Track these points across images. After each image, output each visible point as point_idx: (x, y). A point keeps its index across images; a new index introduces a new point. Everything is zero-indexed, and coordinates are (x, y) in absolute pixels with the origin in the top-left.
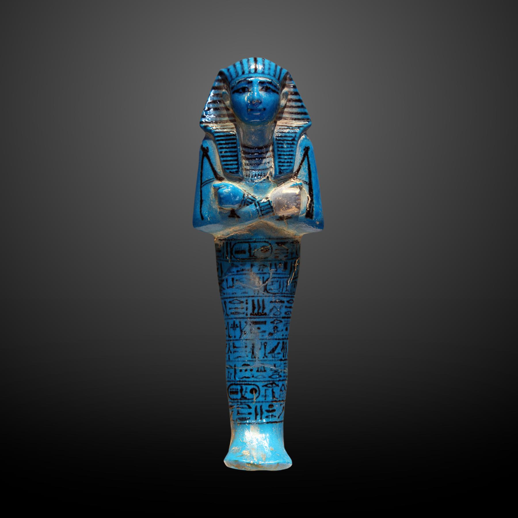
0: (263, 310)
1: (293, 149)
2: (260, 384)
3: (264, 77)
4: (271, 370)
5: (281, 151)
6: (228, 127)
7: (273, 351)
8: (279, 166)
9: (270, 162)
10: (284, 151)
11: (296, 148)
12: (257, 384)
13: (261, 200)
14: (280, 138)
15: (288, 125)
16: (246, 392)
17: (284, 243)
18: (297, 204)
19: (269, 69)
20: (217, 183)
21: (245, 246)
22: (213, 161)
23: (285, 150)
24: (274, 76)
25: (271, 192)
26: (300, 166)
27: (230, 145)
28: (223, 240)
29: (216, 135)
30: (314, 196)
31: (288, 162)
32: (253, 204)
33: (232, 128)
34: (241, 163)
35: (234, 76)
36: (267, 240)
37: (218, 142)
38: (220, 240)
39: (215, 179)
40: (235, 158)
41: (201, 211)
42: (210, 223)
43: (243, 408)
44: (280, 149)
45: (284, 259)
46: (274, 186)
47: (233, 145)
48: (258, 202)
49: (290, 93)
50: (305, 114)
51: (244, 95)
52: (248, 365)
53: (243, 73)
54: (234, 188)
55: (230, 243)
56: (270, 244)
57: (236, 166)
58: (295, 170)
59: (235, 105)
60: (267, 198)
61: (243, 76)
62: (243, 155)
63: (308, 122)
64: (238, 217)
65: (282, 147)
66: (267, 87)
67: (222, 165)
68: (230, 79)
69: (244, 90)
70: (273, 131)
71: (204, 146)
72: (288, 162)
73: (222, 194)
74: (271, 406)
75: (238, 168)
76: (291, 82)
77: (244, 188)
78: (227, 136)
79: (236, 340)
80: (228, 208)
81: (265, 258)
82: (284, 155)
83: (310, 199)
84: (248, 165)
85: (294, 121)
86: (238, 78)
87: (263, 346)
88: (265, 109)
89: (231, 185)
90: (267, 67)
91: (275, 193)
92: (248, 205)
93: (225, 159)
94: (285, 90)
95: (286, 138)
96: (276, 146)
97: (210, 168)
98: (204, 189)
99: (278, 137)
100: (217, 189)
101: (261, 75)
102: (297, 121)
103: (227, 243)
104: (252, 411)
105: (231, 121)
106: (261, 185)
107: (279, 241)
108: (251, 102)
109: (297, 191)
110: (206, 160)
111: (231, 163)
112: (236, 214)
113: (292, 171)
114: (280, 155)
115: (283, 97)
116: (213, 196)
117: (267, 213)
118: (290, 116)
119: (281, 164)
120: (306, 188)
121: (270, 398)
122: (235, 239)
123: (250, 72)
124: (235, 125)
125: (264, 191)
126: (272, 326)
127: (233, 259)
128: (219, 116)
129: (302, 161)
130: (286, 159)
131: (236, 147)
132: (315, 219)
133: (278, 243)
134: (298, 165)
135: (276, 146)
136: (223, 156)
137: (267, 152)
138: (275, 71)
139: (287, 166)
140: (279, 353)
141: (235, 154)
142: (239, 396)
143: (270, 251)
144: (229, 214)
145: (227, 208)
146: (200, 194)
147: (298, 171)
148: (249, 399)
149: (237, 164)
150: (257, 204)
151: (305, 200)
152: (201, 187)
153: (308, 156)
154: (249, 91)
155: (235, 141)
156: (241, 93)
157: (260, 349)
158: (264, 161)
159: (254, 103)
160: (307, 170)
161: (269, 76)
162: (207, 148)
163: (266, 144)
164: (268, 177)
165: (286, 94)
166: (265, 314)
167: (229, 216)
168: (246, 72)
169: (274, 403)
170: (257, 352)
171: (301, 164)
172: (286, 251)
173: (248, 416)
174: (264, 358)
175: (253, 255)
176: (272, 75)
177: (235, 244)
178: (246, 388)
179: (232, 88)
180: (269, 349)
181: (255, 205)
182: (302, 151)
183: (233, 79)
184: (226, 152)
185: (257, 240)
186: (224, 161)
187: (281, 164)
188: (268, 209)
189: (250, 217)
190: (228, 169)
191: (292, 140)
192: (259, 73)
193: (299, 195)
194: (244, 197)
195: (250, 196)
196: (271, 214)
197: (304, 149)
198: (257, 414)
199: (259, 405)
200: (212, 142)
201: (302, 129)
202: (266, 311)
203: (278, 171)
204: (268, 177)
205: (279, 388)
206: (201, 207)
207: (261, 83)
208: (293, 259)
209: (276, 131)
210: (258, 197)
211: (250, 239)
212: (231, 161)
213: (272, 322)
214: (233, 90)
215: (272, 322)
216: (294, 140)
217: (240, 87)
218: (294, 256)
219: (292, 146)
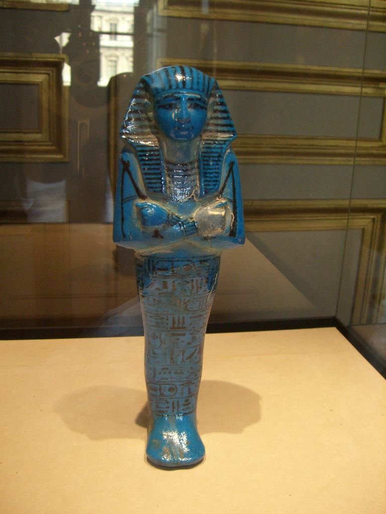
0: (182, 325)
2: (177, 384)
3: (193, 93)
4: (188, 372)
8: (205, 185)
10: (210, 169)
11: (222, 165)
12: (175, 383)
14: (206, 155)
16: (164, 390)
17: (205, 261)
19: (198, 83)
20: (140, 202)
22: (134, 177)
23: (211, 167)
24: (203, 90)
25: (196, 212)
30: (238, 214)
31: (214, 181)
36: (190, 259)
38: (141, 255)
41: (122, 229)
43: (161, 403)
50: (231, 126)
51: (171, 112)
52: (167, 369)
55: (153, 261)
60: (192, 218)
61: (170, 91)
64: (162, 237)
65: (208, 165)
66: (196, 104)
69: (170, 107)
71: (124, 159)
72: (214, 181)
73: (147, 216)
74: (187, 401)
79: (156, 348)
80: (151, 229)
82: (210, 173)
83: (234, 217)
85: (219, 134)
87: (181, 353)
89: (155, 205)
90: (195, 80)
93: (148, 176)
95: (212, 155)
98: (125, 205)
99: (204, 153)
100: (141, 209)
101: (190, 91)
103: (149, 260)
104: (170, 405)
105: (153, 133)
107: (201, 259)
108: (178, 121)
110: (126, 175)
111: (156, 181)
112: (159, 235)
114: (206, 173)
123: (178, 87)
124: (158, 139)
125: (190, 211)
128: (141, 127)
130: (211, 177)
133: (201, 262)
135: (202, 164)
136: (146, 174)
138: (204, 85)
139: (214, 185)
142: (158, 393)
144: (152, 234)
146: (121, 211)
147: (223, 188)
148: (167, 396)
152: (122, 204)
153: (232, 171)
154: (176, 108)
156: (167, 109)
157: (178, 355)
160: (231, 186)
161: (197, 92)
162: (128, 161)
163: (191, 159)
164: (193, 197)
166: (185, 328)
167: (153, 236)
168: (174, 87)
171: (226, 181)
172: (208, 268)
174: (181, 362)
176: (201, 90)
177: (158, 262)
178: (165, 387)
179: (158, 102)
184: (149, 169)
186: (148, 179)
187: (207, 183)
188: (192, 230)
189: (174, 236)
194: (168, 217)
195: (174, 217)
196: (196, 234)
197: (229, 165)
198: (174, 408)
199: (176, 401)
204: (193, 197)
206: (122, 224)
207: (190, 99)
212: (154, 179)
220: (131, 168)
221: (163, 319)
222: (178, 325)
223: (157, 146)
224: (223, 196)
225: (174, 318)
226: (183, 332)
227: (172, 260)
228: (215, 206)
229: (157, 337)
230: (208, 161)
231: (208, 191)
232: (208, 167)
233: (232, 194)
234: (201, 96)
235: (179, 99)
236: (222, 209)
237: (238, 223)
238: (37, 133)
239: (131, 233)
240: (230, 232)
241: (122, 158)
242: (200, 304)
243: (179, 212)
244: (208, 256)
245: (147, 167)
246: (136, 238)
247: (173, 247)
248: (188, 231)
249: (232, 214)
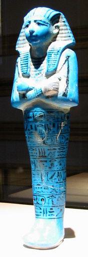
2: (46, 196)
7: (52, 178)
9: (44, 65)
30: (69, 84)
40: (26, 65)
104: (42, 211)
121: (51, 205)
126: (50, 163)
133: (48, 112)
134: (61, 66)
140: (55, 179)
169: (53, 208)
170: (43, 178)
173: (40, 214)
180: (50, 176)
202: (46, 155)
205: (56, 199)
208: (58, 121)
213: (50, 161)
215: (50, 161)
226: (45, 160)
237: (69, 89)
242: (52, 140)
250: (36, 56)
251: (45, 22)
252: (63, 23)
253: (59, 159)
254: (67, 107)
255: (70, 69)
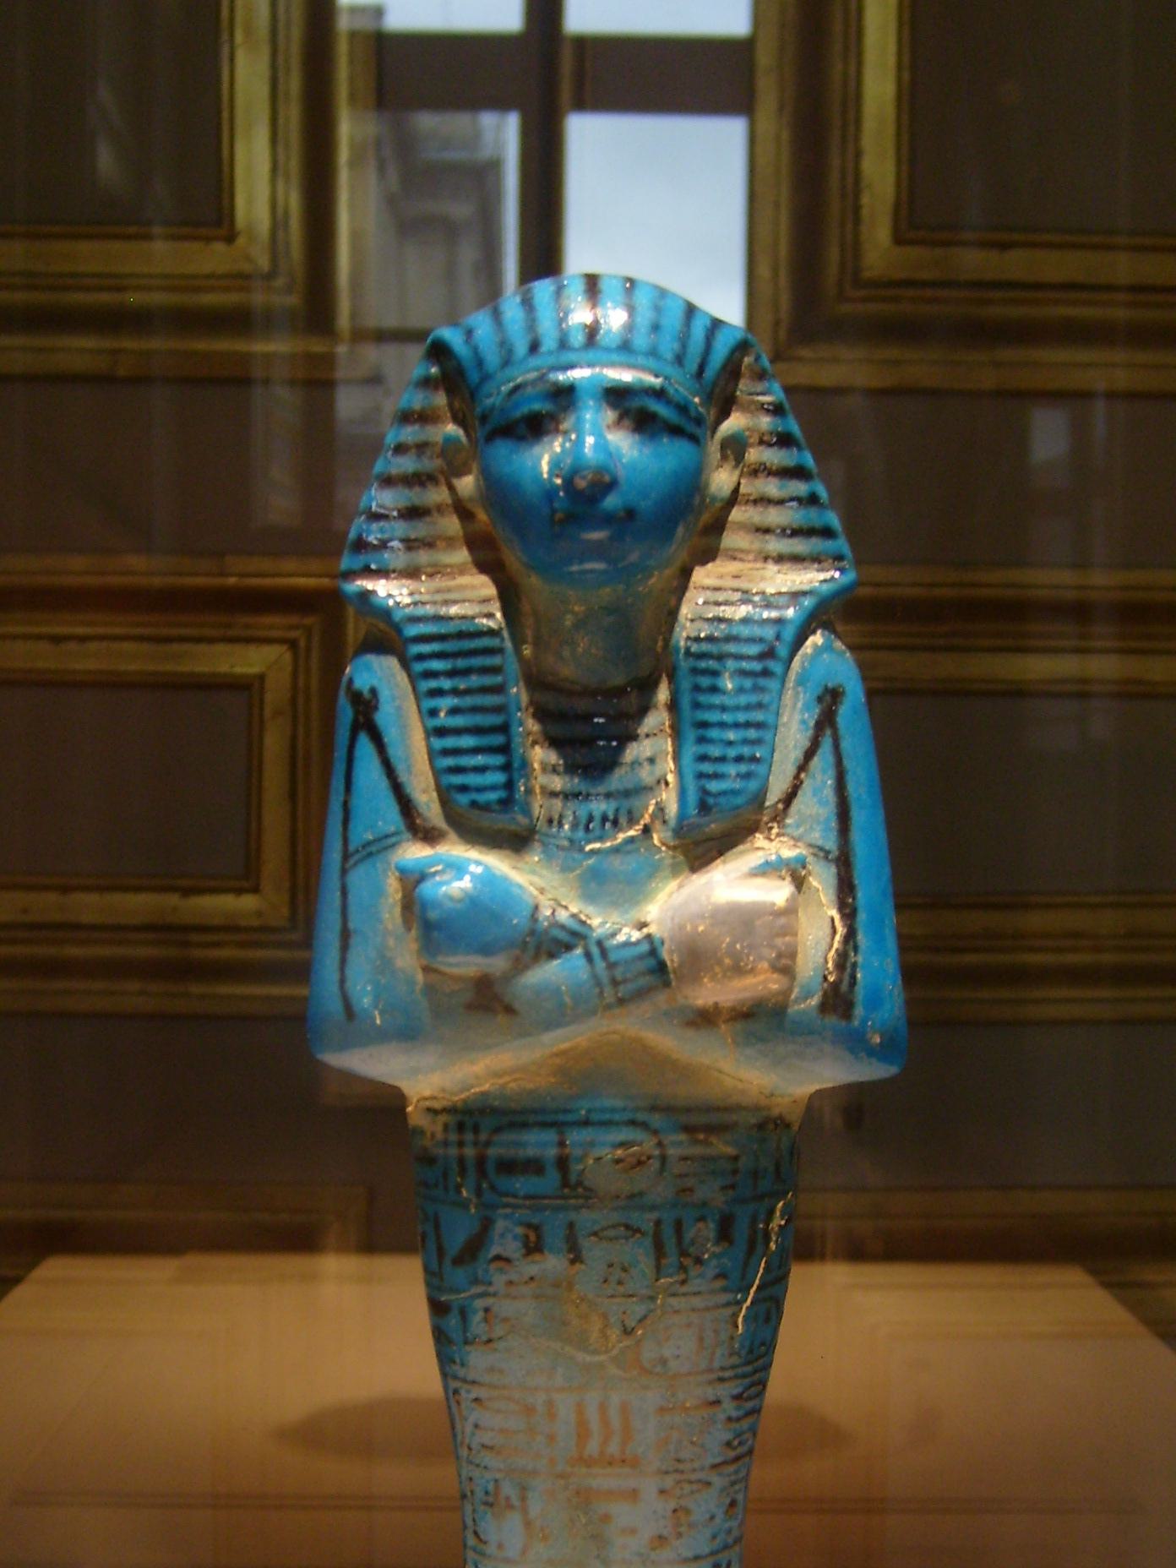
1: (766, 699)
5: (711, 707)
6: (468, 594)
9: (655, 755)
10: (724, 709)
13: (614, 935)
15: (744, 585)
18: (780, 956)
19: (656, 328)
20: (414, 853)
21: (538, 1143)
22: (394, 752)
24: (679, 360)
26: (797, 777)
27: (475, 681)
28: (445, 1110)
29: (412, 631)
30: (862, 917)
31: (739, 759)
32: (579, 951)
33: (485, 601)
34: (525, 764)
35: (492, 359)
36: (640, 1117)
37: (419, 667)
38: (429, 1110)
39: (408, 835)
40: (497, 740)
41: (342, 981)
42: (382, 1036)
44: (703, 699)
45: (719, 1200)
46: (675, 871)
47: (489, 680)
48: (600, 943)
49: (754, 439)
51: (537, 450)
53: (534, 347)
54: (488, 879)
56: (655, 1132)
57: (499, 778)
58: (773, 797)
59: (498, 492)
60: (644, 925)
61: (535, 362)
62: (533, 726)
63: (842, 570)
64: (510, 1010)
65: (714, 689)
67: (437, 773)
68: (474, 377)
69: (536, 427)
70: (673, 614)
72: (739, 759)
73: (437, 904)
75: (509, 786)
76: (760, 387)
77: (536, 879)
78: (461, 635)
80: (464, 965)
81: (632, 1196)
82: (722, 725)
84: (554, 770)
85: (772, 568)
86: (508, 372)
88: (630, 514)
89: (478, 863)
91: (674, 904)
92: (552, 956)
94: (734, 423)
95: (732, 648)
96: (685, 684)
97: (383, 784)
98: (358, 878)
99: (697, 639)
101: (615, 357)
102: (786, 566)
103: (461, 1127)
105: (483, 567)
106: (616, 862)
108: (569, 483)
109: (778, 893)
110: (365, 746)
111: (480, 760)
113: (759, 798)
114: (704, 725)
115: (724, 457)
116: (398, 910)
117: (640, 994)
118: (757, 545)
119: (707, 768)
120: (822, 882)
122: (495, 1111)
123: (563, 344)
125: (632, 890)
127: (488, 1196)
129: (809, 754)
130: (730, 743)
131: (499, 689)
132: (864, 1021)
134: (791, 770)
136: (441, 732)
137: (644, 710)
138: (684, 339)
141: (496, 720)
143: (655, 1165)
145: (456, 971)
147: (789, 799)
149: (506, 767)
150: (595, 951)
151: (818, 935)
152: (344, 872)
154: (557, 431)
155: (495, 661)
156: (522, 439)
158: (632, 752)
159: (581, 484)
160: (829, 793)
161: (651, 363)
162: (373, 691)
164: (647, 830)
165: (735, 448)
167: (471, 1007)
168: (549, 343)
171: (802, 767)
175: (580, 1184)
176: (669, 356)
179: (484, 418)
181: (588, 956)
182: (806, 707)
183: (486, 378)
184: (454, 711)
185: (595, 1117)
186: (446, 752)
187: (707, 768)
190: (464, 789)
191: (762, 657)
192: (608, 350)
193: (790, 910)
195: (563, 916)
197: (820, 699)
200: (392, 663)
201: (807, 602)
203: (692, 798)
204: (647, 830)
206: (343, 962)
207: (616, 395)
208: (760, 1198)
209: (685, 611)
210: (599, 921)
211: (566, 1111)
212: (476, 751)
214: (488, 427)
216: (771, 658)
217: (518, 414)
218: (765, 1185)
219: (762, 682)
220: (385, 717)
221: (530, 1410)
222: (605, 1441)
223: (490, 616)
224: (789, 830)
225: (580, 1408)
227: (561, 1117)
228: (745, 869)
229: (510, 1507)
230: (715, 674)
231: (711, 801)
232: (716, 700)
233: (834, 824)
234: (666, 378)
235: (565, 396)
236: (779, 883)
237: (860, 959)
238: (239, 891)
239: (377, 999)
240: (825, 995)
241: (351, 681)
243: (589, 897)
244: (728, 1109)
245: (446, 703)
246: (406, 1033)
247: (558, 1061)
248: (625, 981)
249: (834, 913)
250: (567, 671)
251: (683, 409)
252: (765, 422)
253: (731, 1469)
254: (792, 1080)
255: (852, 788)
